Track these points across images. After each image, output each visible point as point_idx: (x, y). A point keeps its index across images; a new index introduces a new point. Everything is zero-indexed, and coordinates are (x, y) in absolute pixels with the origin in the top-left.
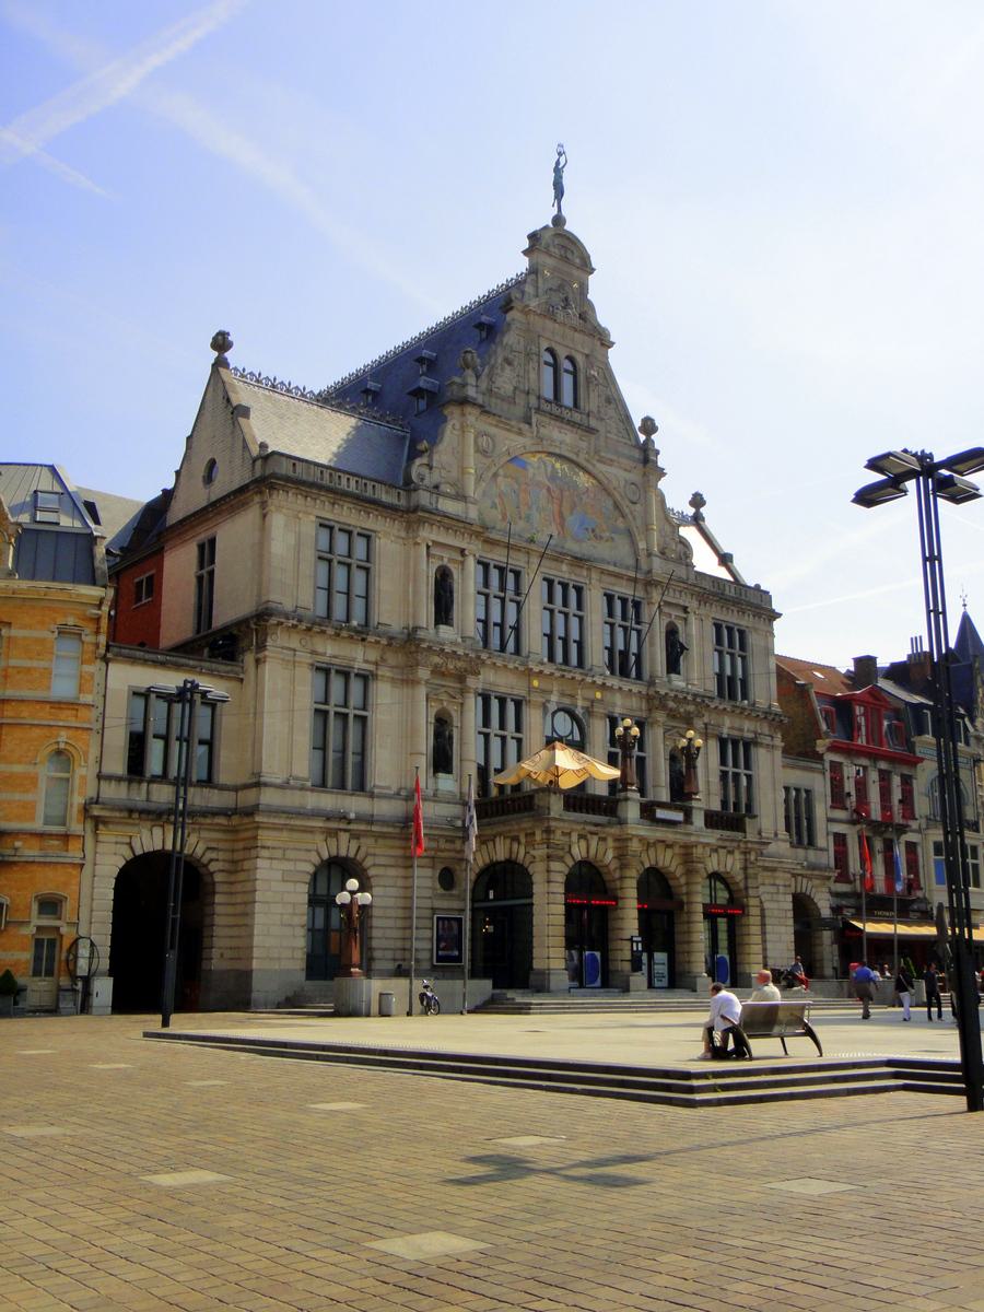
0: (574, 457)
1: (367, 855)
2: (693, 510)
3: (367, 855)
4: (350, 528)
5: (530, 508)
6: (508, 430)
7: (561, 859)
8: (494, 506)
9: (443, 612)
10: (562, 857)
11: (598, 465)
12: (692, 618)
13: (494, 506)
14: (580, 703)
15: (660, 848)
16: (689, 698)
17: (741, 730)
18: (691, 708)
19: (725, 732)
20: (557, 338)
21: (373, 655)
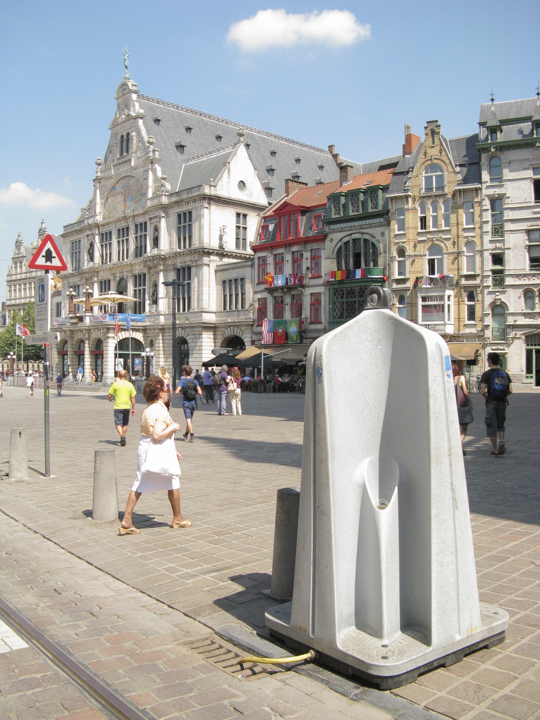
14: (125, 274)
17: (185, 262)
20: (122, 130)
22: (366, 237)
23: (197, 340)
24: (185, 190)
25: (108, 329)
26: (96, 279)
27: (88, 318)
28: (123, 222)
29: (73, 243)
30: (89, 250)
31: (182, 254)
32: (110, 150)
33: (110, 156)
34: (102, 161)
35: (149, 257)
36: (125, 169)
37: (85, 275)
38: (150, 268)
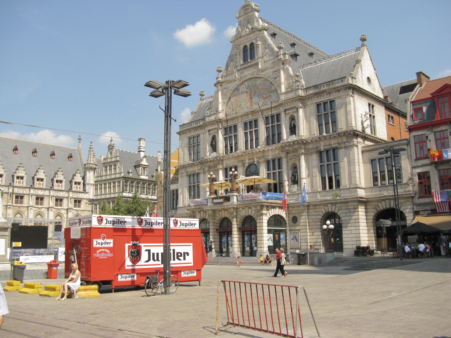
0: (253, 76)
9: (214, 147)
11: (260, 73)
13: (230, 108)
14: (256, 160)
15: (223, 212)
16: (292, 143)
17: (331, 145)
19: (322, 149)
20: (245, 41)
23: (352, 214)
24: (325, 83)
25: (262, 206)
26: (221, 167)
27: (235, 197)
28: (250, 116)
29: (190, 138)
30: (212, 142)
31: (328, 137)
32: (231, 58)
33: (232, 63)
34: (223, 68)
35: (290, 142)
37: (209, 164)
38: (287, 153)
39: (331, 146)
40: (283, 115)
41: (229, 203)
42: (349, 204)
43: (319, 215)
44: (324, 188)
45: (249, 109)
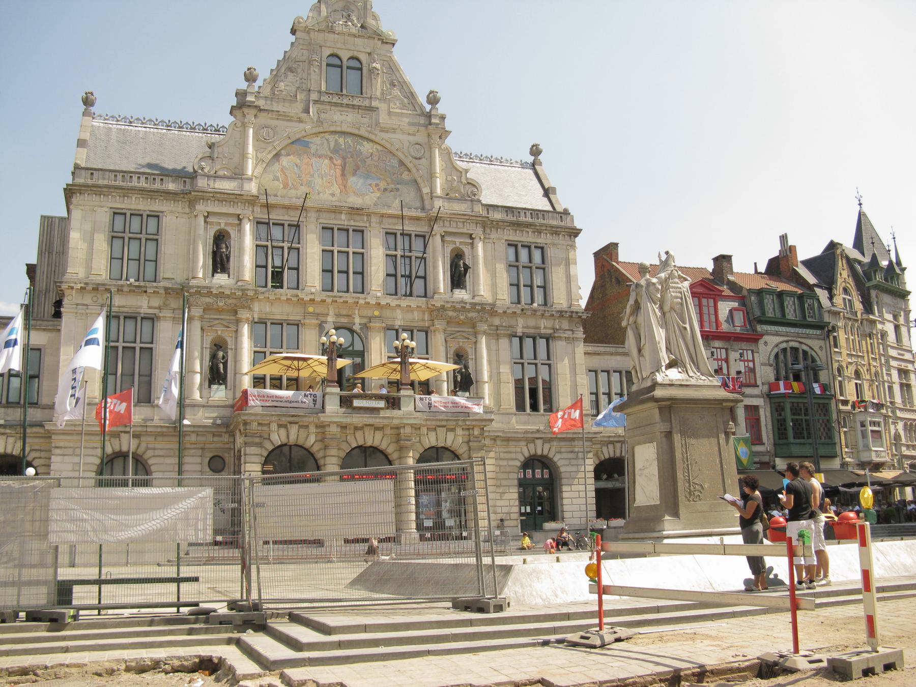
0: (356, 132)
1: (147, 449)
2: (533, 158)
3: (147, 449)
4: (140, 213)
5: (312, 176)
6: (288, 120)
7: (260, 445)
8: (278, 180)
9: (220, 262)
10: (261, 443)
11: (380, 134)
12: (480, 247)
13: (276, 179)
14: (357, 320)
16: (468, 306)
17: (539, 328)
18: (474, 315)
19: (519, 331)
20: (339, 45)
21: (156, 302)
22: (805, 348)
23: (581, 462)
24: (528, 210)
28: (343, 217)
29: (115, 213)
31: (539, 313)
34: (264, 74)
35: (466, 303)
36: (344, 117)
37: (208, 300)
39: (537, 331)
40: (436, 242)
41: (396, 413)
42: (576, 443)
43: (516, 459)
44: (520, 407)
45: (335, 199)
